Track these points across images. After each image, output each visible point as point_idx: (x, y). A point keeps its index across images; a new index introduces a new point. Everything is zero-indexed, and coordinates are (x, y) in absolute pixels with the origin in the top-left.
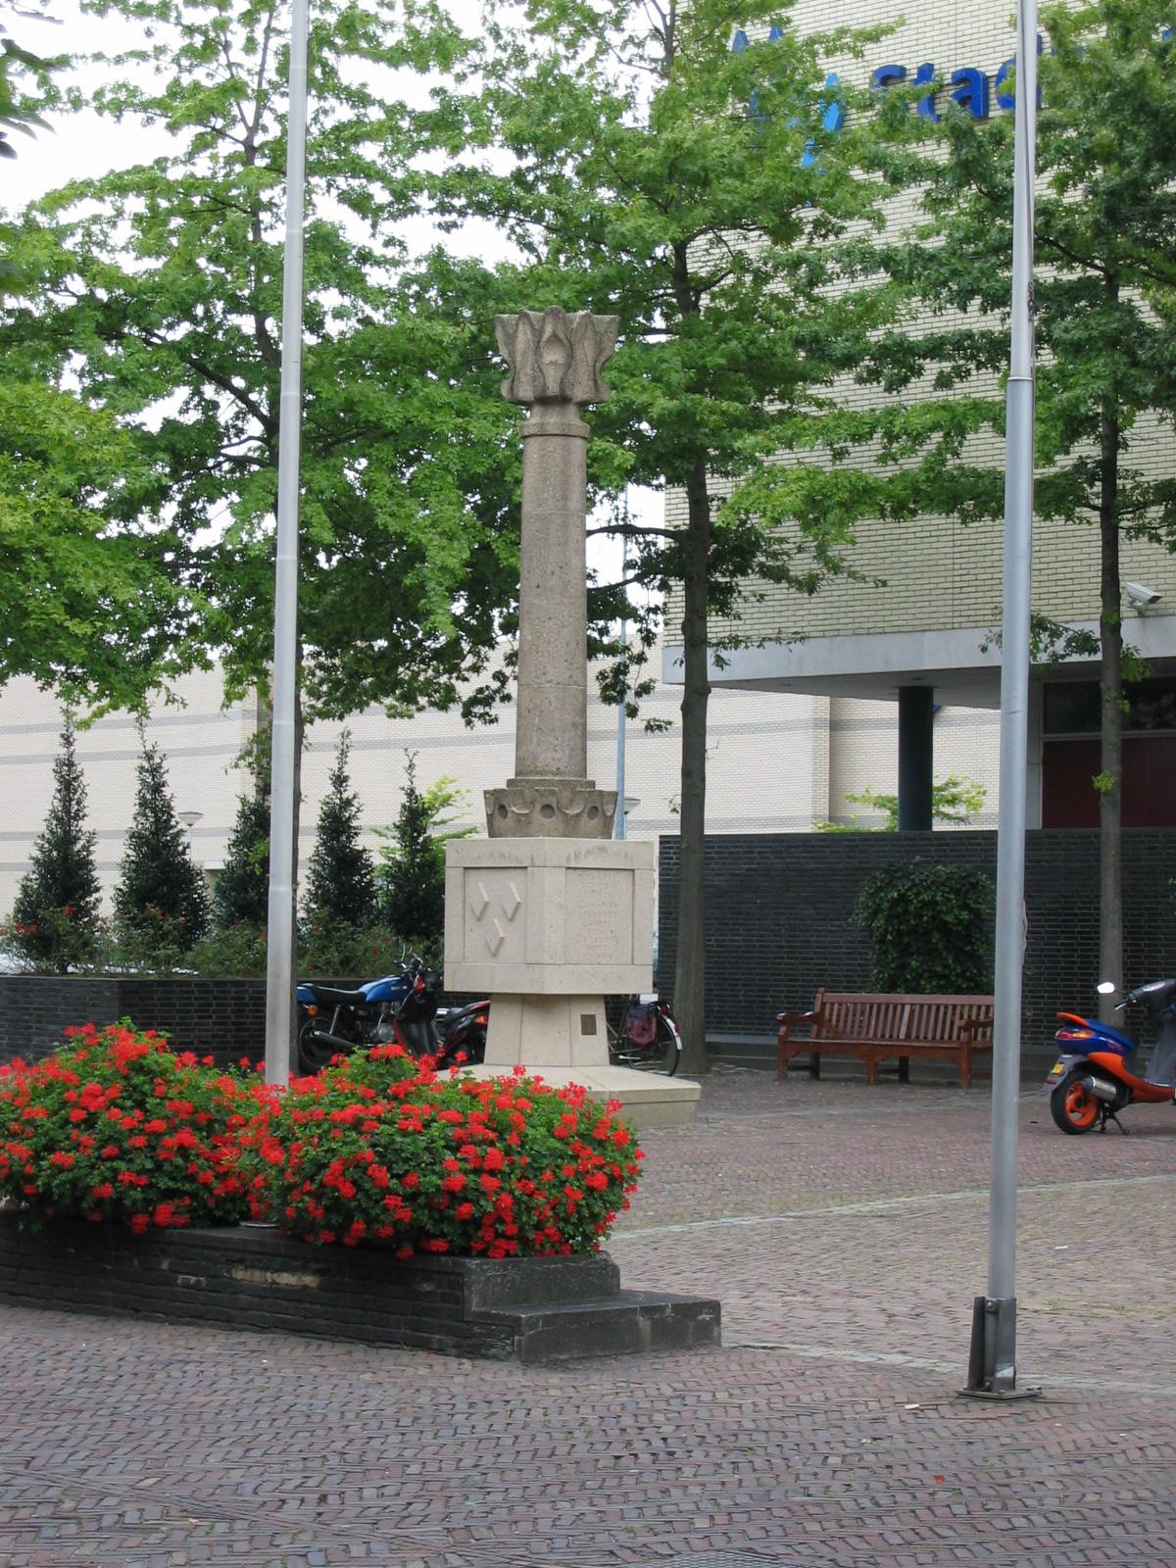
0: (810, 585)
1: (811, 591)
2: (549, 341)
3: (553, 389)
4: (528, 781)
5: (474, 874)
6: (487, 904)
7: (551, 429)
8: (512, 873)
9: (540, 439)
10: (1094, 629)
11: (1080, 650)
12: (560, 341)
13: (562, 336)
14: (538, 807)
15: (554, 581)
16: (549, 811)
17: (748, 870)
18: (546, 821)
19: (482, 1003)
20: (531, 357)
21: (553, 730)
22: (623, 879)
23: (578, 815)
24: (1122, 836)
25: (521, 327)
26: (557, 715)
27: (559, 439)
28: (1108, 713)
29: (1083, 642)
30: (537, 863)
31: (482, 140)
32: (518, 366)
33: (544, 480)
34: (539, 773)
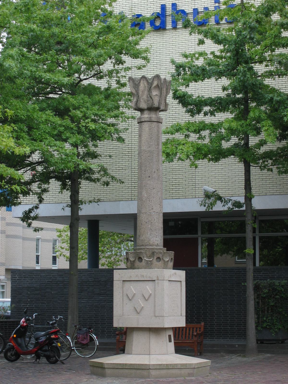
0: (107, 184)
1: (107, 185)
2: (155, 87)
3: (156, 104)
4: (148, 248)
5: (127, 284)
6: (135, 294)
7: (153, 119)
8: (147, 282)
9: (149, 123)
10: (242, 200)
11: (236, 207)
12: (159, 87)
13: (159, 85)
14: (155, 258)
15: (155, 175)
16: (159, 260)
17: (48, 281)
18: (158, 263)
19: (125, 333)
20: (146, 92)
21: (156, 230)
22: (179, 283)
23: (168, 261)
24: (254, 269)
25: (142, 82)
26: (157, 224)
27: (156, 123)
28: (249, 229)
29: (237, 204)
30: (160, 279)
31: (34, 23)
32: (140, 96)
33: (151, 138)
34: (150, 245)
